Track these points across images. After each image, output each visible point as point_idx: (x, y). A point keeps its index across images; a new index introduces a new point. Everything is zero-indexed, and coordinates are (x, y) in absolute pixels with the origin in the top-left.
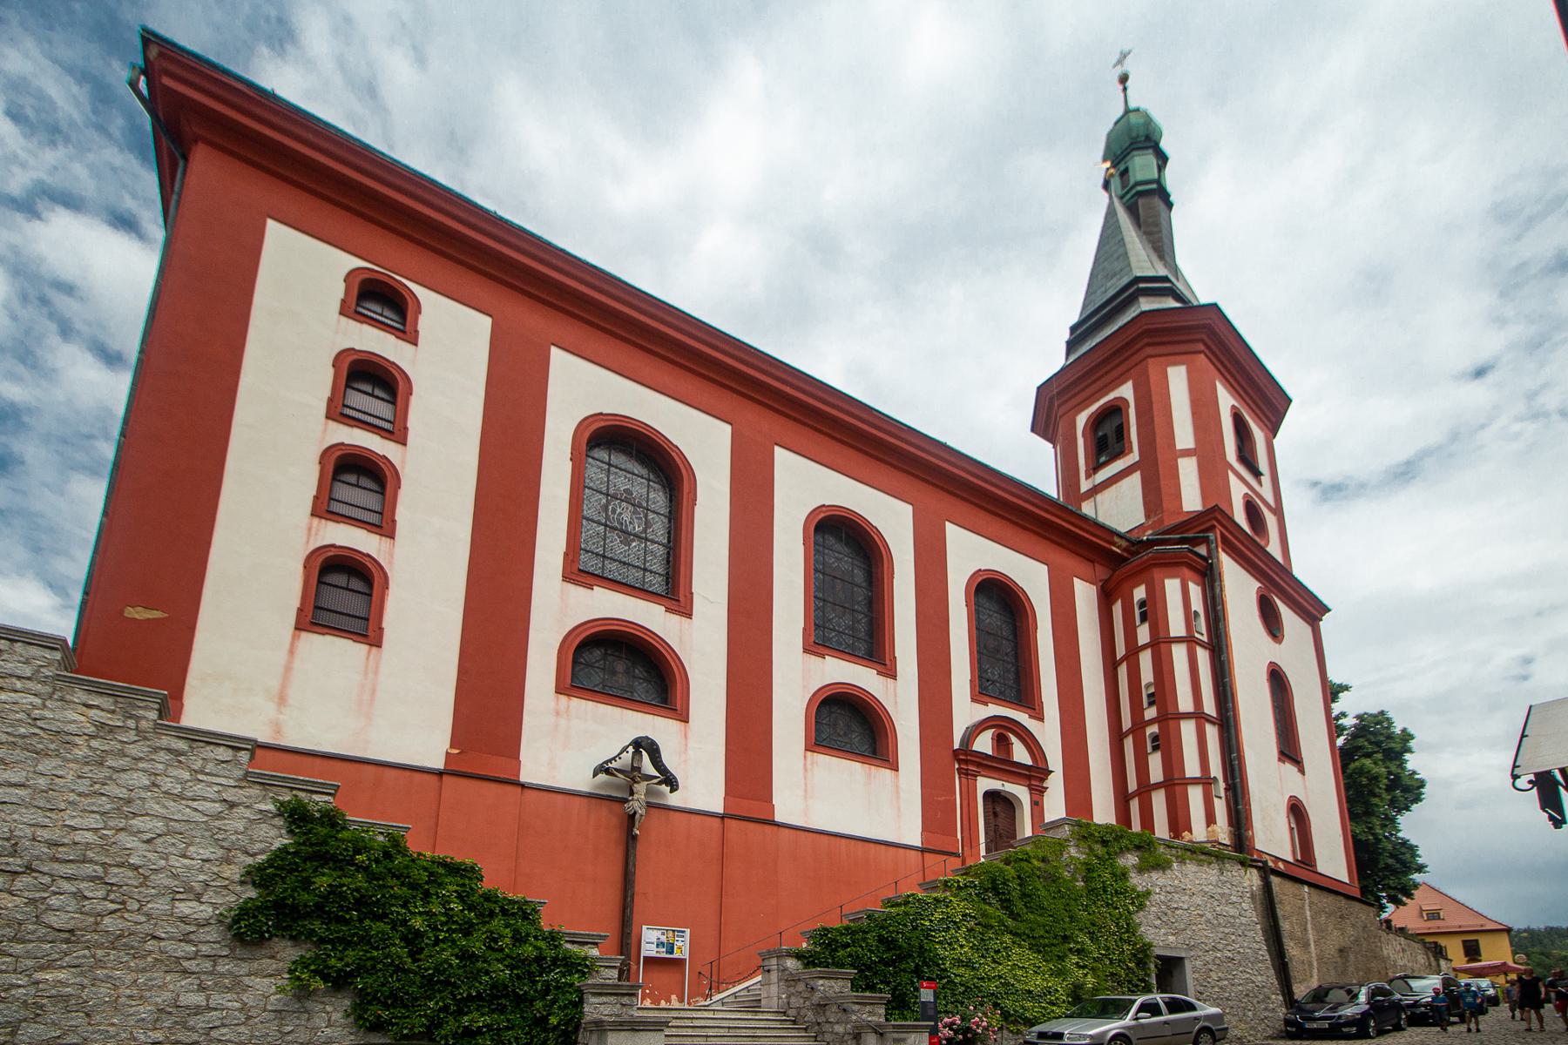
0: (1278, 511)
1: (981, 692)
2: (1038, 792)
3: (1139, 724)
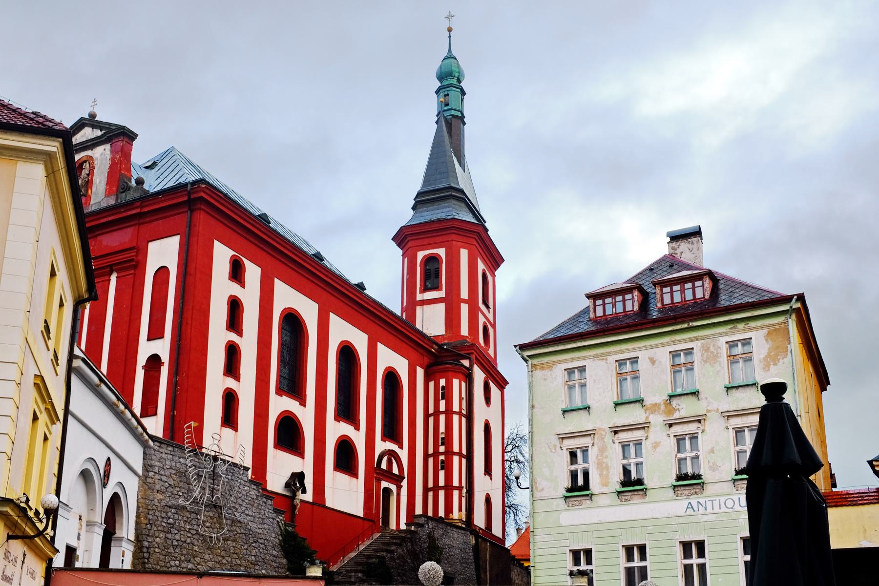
0: (494, 326)
1: (386, 437)
3: (436, 454)
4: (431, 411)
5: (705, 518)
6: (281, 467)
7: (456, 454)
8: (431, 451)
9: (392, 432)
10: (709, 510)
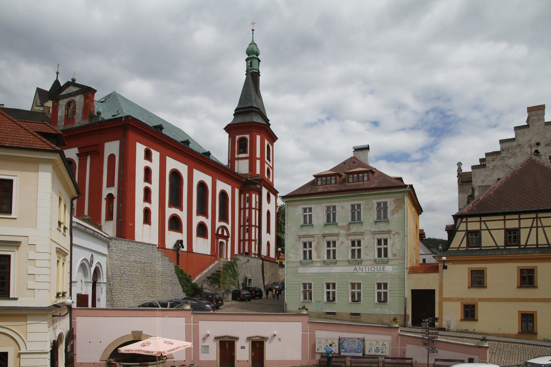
1: (220, 220)
2: (227, 241)
3: (244, 226)
4: (242, 207)
5: (362, 274)
6: (171, 238)
7: (254, 226)
8: (242, 224)
9: (224, 217)
10: (364, 271)
